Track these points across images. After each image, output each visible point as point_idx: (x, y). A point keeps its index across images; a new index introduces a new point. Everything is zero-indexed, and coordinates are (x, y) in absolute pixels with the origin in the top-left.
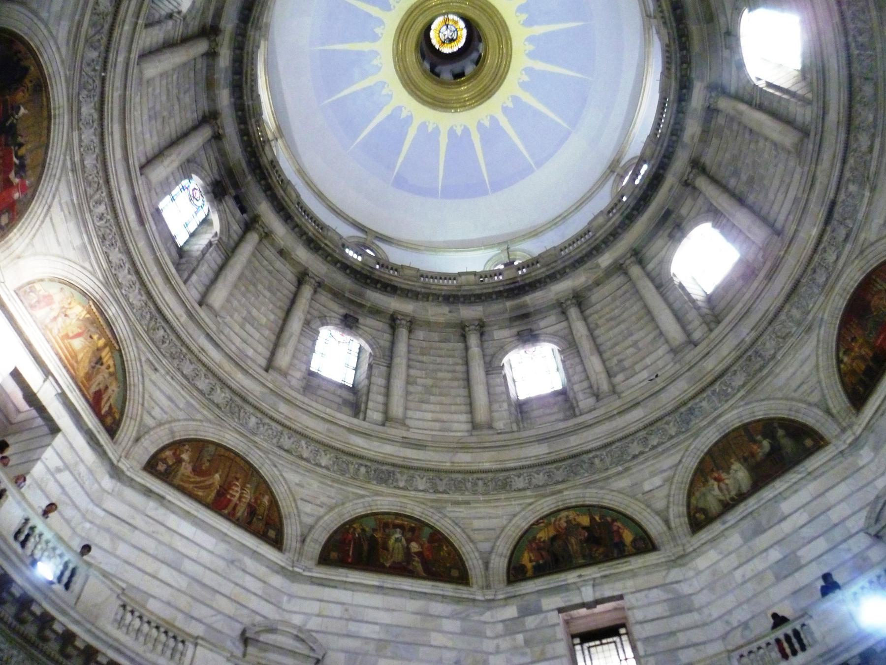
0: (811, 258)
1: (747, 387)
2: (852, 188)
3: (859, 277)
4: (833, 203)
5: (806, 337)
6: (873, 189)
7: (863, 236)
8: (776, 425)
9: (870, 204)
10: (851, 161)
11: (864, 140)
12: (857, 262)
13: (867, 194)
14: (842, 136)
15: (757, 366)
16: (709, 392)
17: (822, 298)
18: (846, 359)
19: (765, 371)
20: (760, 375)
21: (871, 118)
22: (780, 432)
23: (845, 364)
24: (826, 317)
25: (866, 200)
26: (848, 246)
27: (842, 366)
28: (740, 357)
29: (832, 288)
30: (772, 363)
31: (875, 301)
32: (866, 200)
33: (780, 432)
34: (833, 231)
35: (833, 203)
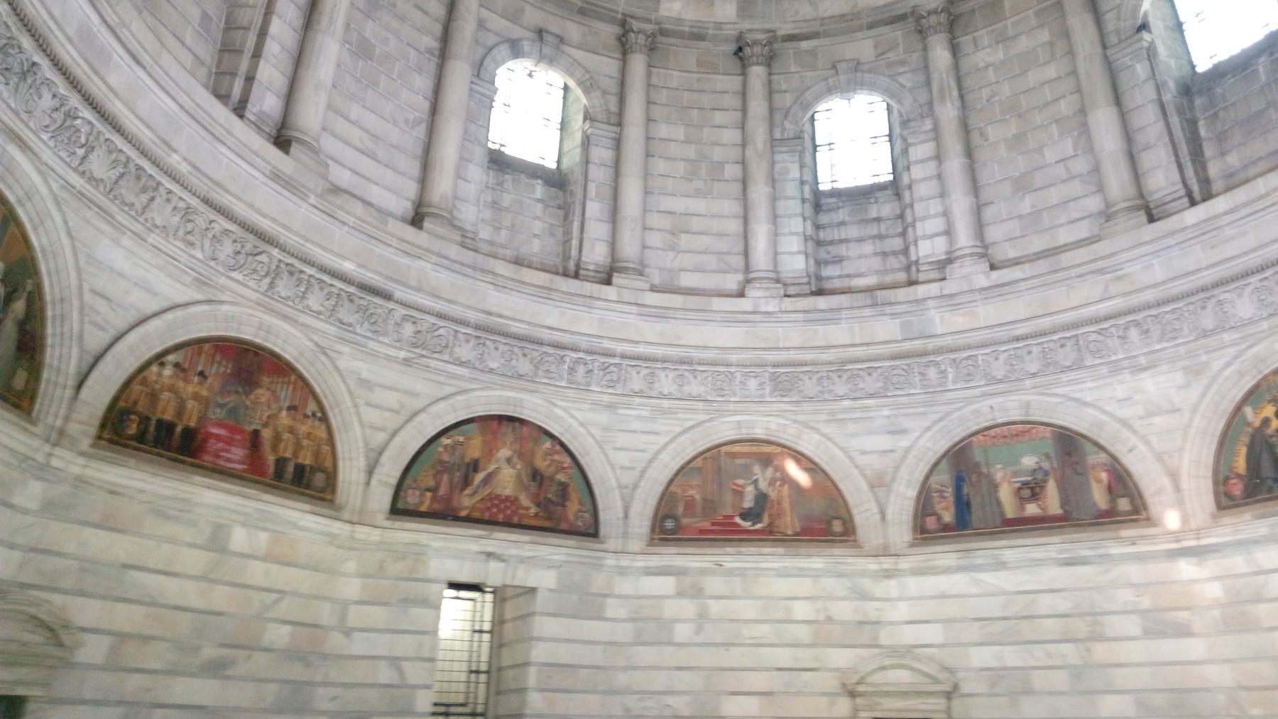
0: (312, 264)
1: (89, 189)
2: (408, 329)
3: (289, 354)
4: (387, 297)
5: (188, 280)
6: (406, 362)
7: (346, 349)
8: (29, 288)
9: (388, 358)
10: (445, 329)
11: (465, 351)
12: (310, 344)
13: (402, 354)
14: (472, 316)
15: (130, 198)
16: (74, 101)
17: (255, 296)
18: (168, 372)
19: (121, 218)
20: (114, 209)
21: (493, 365)
22: (19, 306)
23: (160, 375)
24: (225, 308)
25: (393, 352)
26: (331, 329)
27: (154, 368)
28: (144, 153)
29: (271, 311)
30: (137, 227)
31: (262, 394)
32: (393, 352)
33: (19, 306)
34: (350, 299)
35: (387, 297)
